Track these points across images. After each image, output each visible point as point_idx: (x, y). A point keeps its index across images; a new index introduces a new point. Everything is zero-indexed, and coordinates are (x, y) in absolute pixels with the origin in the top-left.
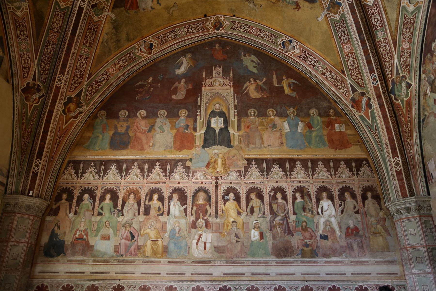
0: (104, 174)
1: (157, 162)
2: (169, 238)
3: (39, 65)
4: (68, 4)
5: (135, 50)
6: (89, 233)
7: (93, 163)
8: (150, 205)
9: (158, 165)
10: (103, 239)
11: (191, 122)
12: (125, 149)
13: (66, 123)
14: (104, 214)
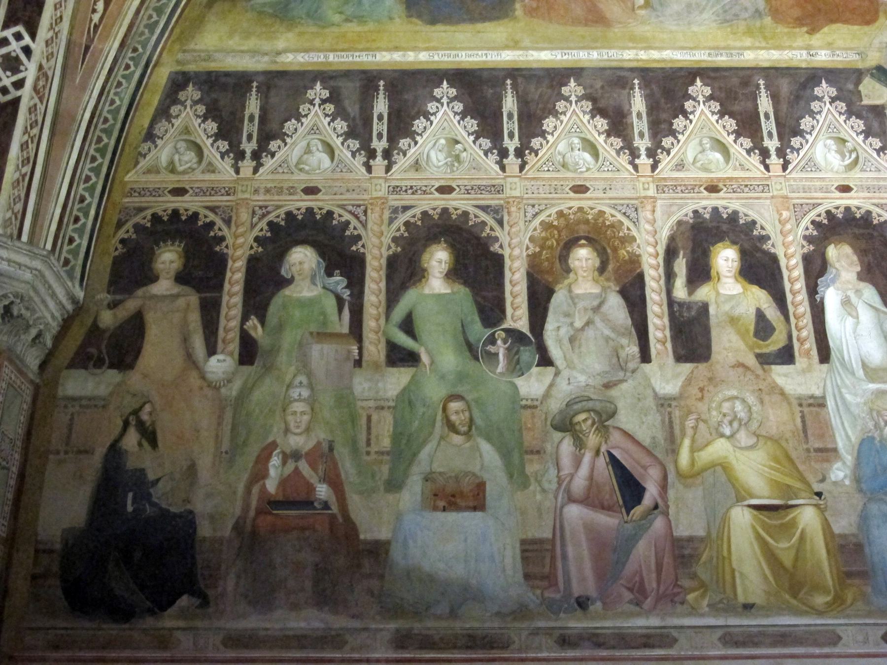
0: (393, 139)
1: (692, 82)
2: (861, 491)
6: (348, 468)
7: (318, 86)
8: (704, 308)
9: (701, 99)
10: (441, 504)
12: (498, 18)
14: (425, 358)
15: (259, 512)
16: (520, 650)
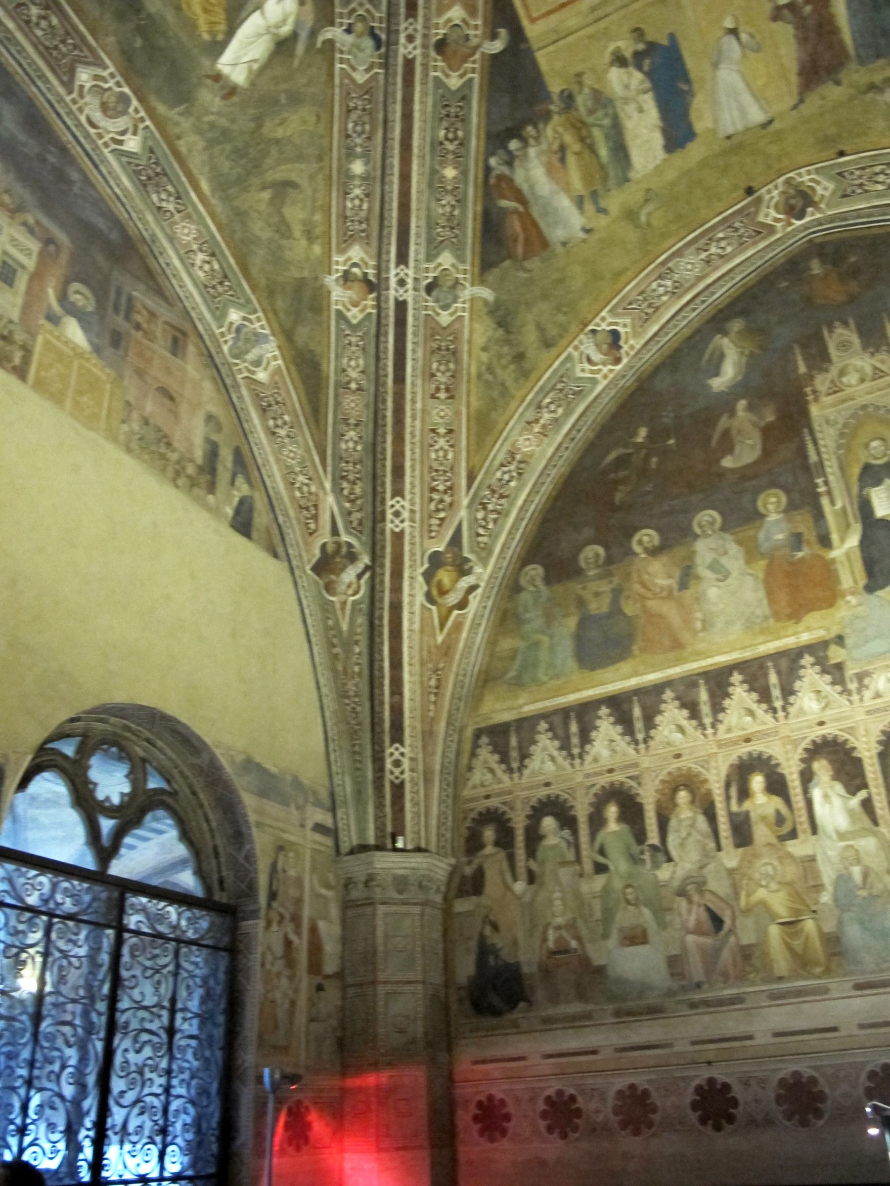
0: (582, 746)
1: (731, 675)
2: (837, 906)
3: (338, 490)
4: (365, 307)
5: (574, 366)
6: (584, 932)
8: (747, 815)
9: (737, 684)
11: (804, 524)
13: (442, 625)
14: (612, 868)
15: (548, 958)
16: (672, 1012)
